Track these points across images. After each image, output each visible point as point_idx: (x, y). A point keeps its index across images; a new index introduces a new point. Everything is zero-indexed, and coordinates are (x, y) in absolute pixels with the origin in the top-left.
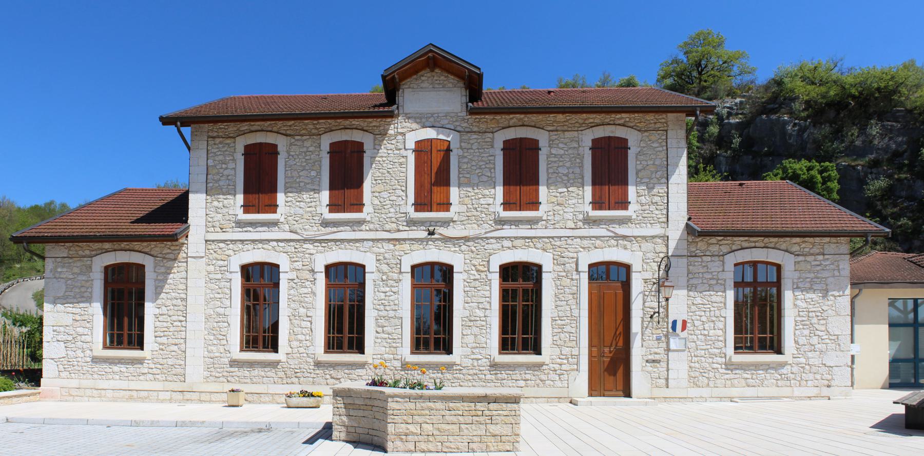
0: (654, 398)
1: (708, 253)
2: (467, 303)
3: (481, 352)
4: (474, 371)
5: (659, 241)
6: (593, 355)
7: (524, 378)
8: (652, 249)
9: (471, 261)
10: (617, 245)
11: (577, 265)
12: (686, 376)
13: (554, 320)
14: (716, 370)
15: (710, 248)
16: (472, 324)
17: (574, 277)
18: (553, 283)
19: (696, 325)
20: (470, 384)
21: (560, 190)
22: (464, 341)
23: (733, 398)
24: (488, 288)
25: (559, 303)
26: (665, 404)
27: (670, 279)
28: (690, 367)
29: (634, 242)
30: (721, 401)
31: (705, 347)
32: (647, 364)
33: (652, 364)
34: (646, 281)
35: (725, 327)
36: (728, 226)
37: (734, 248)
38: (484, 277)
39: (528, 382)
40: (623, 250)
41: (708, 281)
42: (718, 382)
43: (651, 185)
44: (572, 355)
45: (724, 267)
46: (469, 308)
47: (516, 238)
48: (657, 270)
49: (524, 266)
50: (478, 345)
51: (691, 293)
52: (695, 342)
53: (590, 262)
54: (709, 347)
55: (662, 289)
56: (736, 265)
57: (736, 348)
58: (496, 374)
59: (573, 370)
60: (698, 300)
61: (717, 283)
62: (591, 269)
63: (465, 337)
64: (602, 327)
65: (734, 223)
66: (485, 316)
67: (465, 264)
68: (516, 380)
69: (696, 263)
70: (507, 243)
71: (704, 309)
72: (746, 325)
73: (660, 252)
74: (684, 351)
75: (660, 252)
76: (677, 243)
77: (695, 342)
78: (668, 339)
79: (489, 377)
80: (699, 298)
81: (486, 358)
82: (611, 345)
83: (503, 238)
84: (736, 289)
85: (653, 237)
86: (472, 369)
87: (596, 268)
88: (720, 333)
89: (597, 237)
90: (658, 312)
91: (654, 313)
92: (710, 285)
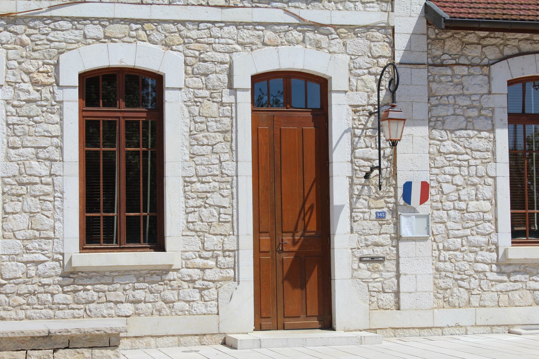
0: (375, 330)
1: (462, 60)
2: (13, 148)
3: (44, 247)
4: (30, 288)
5: (379, 35)
6: (263, 249)
7: (131, 299)
8: (366, 50)
9: (20, 63)
10: (303, 41)
11: (230, 76)
12: (431, 287)
13: (187, 182)
14: (482, 275)
15: (466, 52)
16: (23, 190)
17: (225, 100)
18: (186, 110)
19: (446, 191)
20: (22, 314)
22: (9, 225)
23: (513, 326)
24: (56, 118)
25: (197, 149)
26: (394, 339)
27: (399, 105)
28: (437, 270)
29: (334, 36)
30: (492, 332)
31: (461, 233)
32: (362, 265)
33: (370, 265)
34: (355, 109)
35: (495, 195)
36: (496, 11)
37: (507, 51)
38: (49, 96)
39: (141, 306)
40: (314, 51)
41: (464, 110)
42: (487, 296)
44: (224, 251)
45: (490, 87)
46: (18, 158)
47: (112, 21)
48: (375, 87)
49: (128, 76)
50: (37, 234)
51: (436, 133)
52: (444, 223)
53: (254, 72)
54: (468, 232)
55: (385, 123)
56: (511, 83)
57: (515, 234)
58: (75, 291)
59: (226, 279)
60: (448, 146)
61: (480, 115)
62: (257, 85)
63: (11, 217)
64: (278, 196)
65: (506, 7)
66: (51, 175)
67: (8, 68)
68: (116, 303)
69: (442, 78)
70: (93, 30)
71: (459, 163)
72: (531, 192)
73: (380, 57)
74: (425, 239)
75: (380, 57)
76: (410, 41)
77: (444, 223)
78: (398, 218)
79: (60, 297)
80: (450, 142)
81: (54, 260)
82: (296, 230)
83: (85, 19)
84: (512, 126)
85: (368, 28)
86: (25, 283)
87: (266, 82)
88: (486, 206)
89: (267, 25)
90: (379, 168)
91: (372, 169)
92: (468, 119)
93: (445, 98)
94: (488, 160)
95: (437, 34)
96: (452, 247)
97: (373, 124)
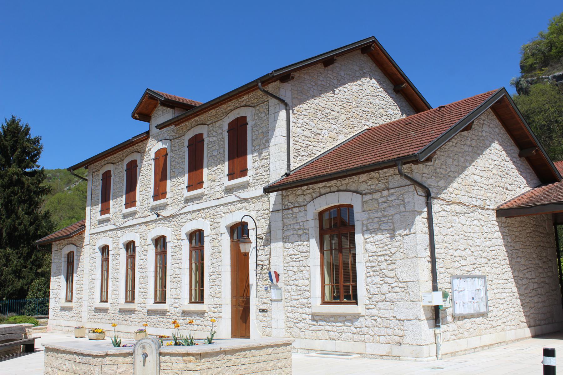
15: (298, 200)
21: (214, 169)
43: (260, 151)
52: (289, 292)
69: (288, 216)
77: (289, 292)
89: (231, 203)
93: (289, 226)
94: (308, 257)
95: (286, 193)
96: (293, 306)
97: (264, 244)
